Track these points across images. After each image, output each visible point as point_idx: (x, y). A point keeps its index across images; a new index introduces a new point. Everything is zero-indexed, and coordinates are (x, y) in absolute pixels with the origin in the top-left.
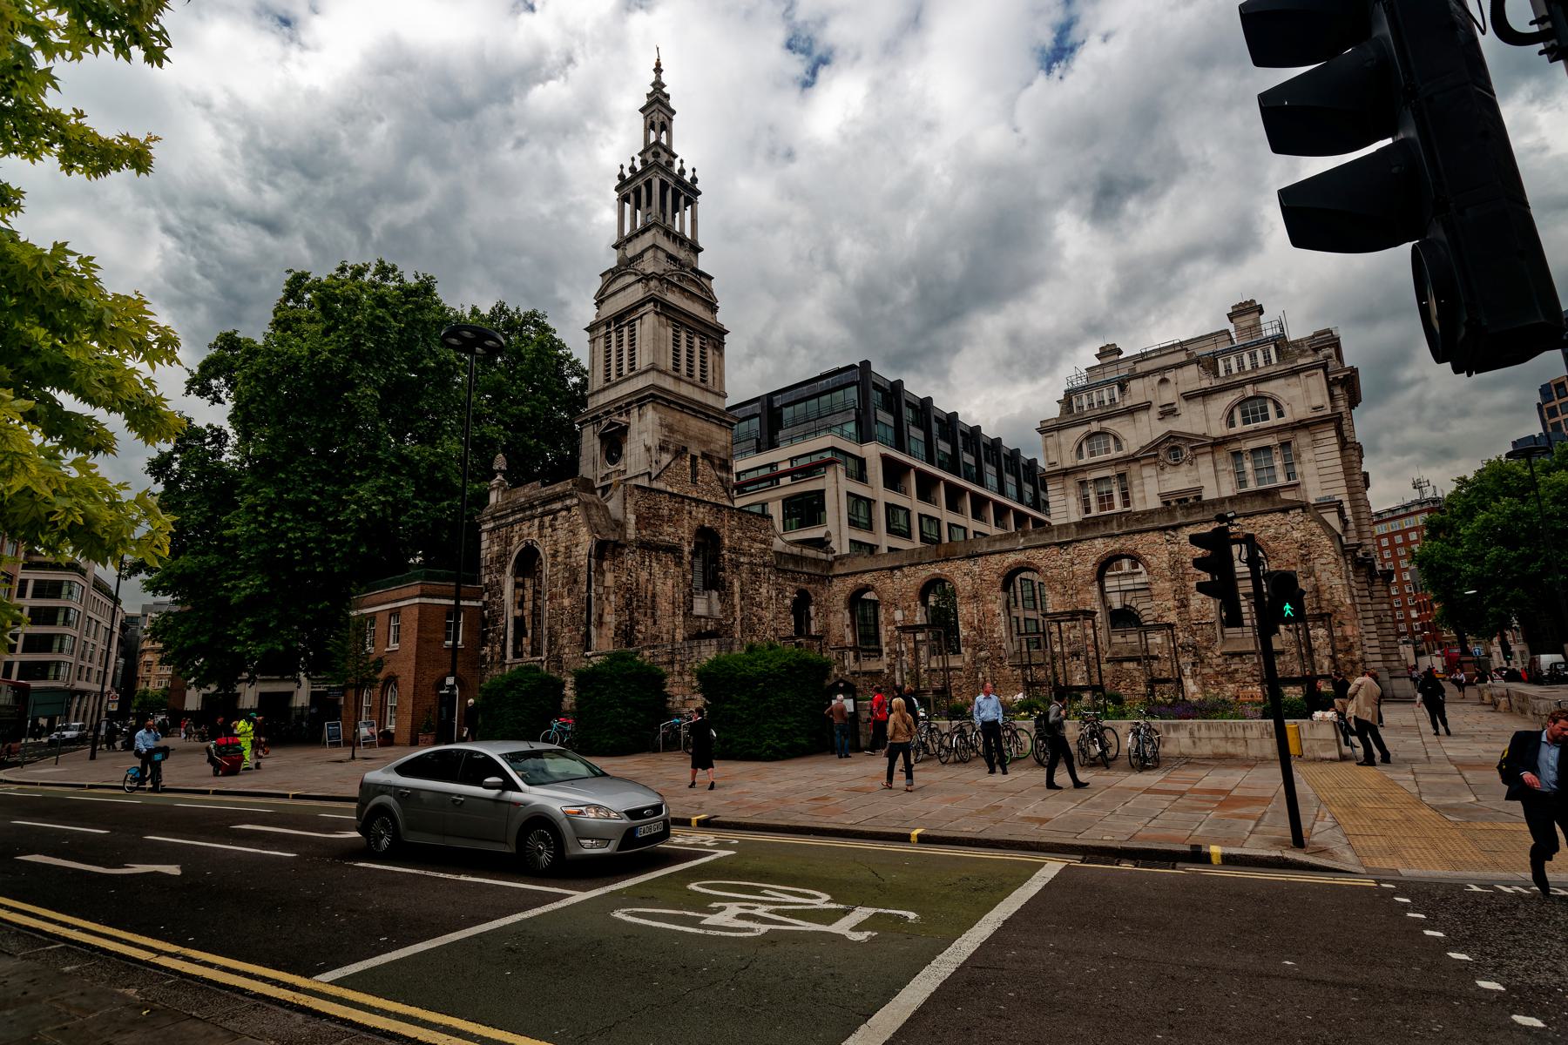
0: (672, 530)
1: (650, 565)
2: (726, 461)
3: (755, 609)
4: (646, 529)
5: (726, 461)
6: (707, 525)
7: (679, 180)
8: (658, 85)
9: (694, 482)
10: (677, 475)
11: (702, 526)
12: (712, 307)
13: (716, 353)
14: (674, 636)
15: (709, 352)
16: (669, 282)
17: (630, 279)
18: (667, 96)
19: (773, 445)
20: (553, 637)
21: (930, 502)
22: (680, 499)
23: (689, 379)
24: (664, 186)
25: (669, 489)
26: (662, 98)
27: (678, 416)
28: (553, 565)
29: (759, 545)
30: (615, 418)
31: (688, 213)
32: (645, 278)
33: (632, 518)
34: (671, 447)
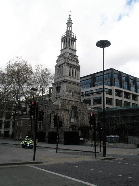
6: (74, 105)
7: (73, 38)
8: (70, 18)
9: (72, 97)
12: (78, 62)
15: (77, 71)
17: (63, 58)
18: (71, 21)
19: (94, 86)
20: (45, 126)
21: (128, 99)
23: (72, 77)
24: (69, 39)
25: (68, 99)
26: (70, 21)
28: (45, 114)
30: (59, 85)
31: (74, 43)
32: (65, 58)
33: (60, 104)
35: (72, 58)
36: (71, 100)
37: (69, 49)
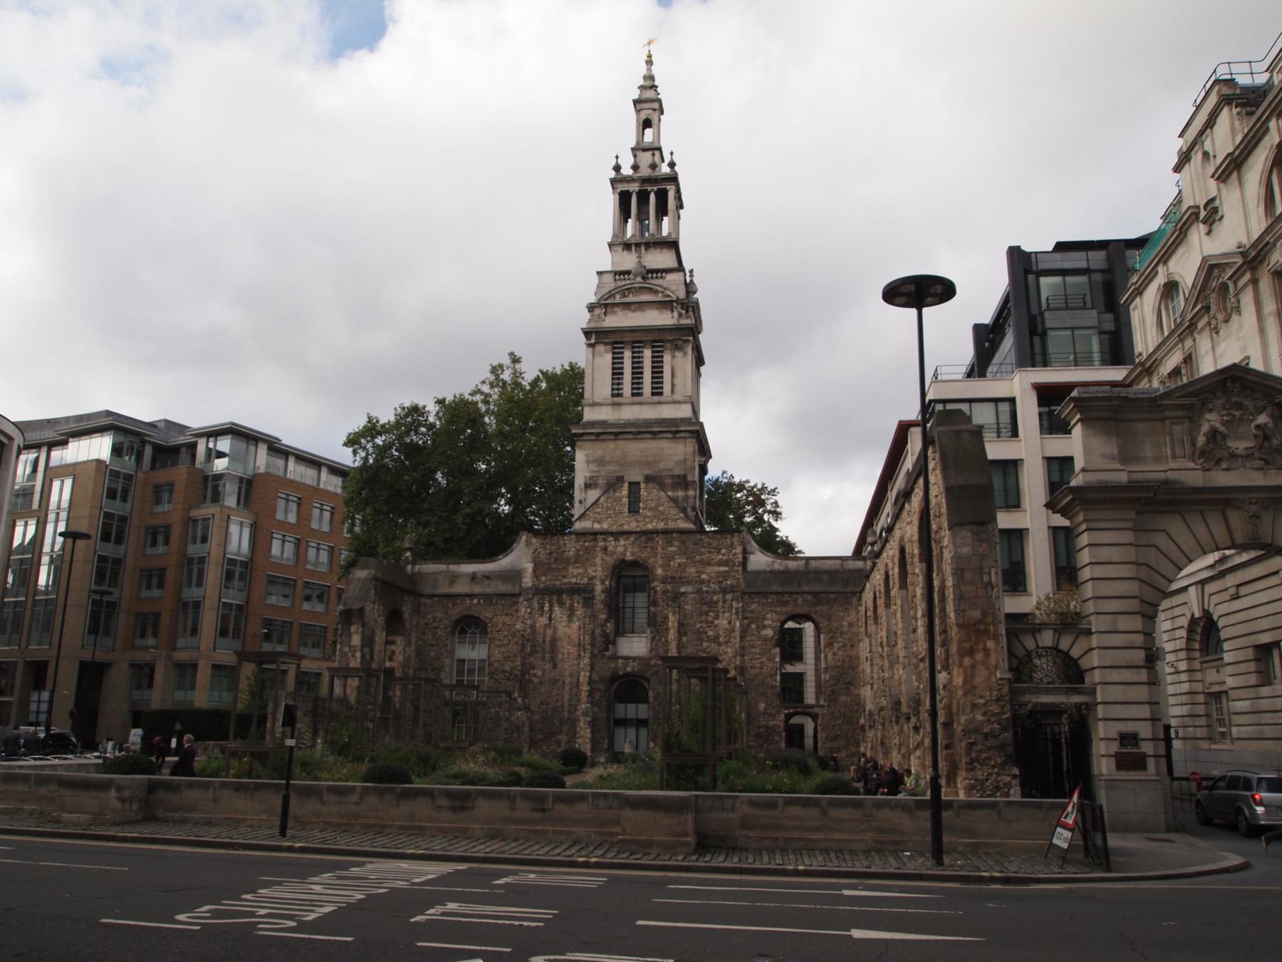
0: (581, 570)
1: (551, 610)
2: (685, 476)
3: (705, 645)
4: (545, 574)
5: (685, 476)
6: (629, 557)
8: (650, 84)
10: (608, 509)
11: (623, 561)
13: (678, 354)
14: (578, 679)
15: (667, 358)
16: (606, 305)
22: (591, 537)
25: (597, 526)
27: (611, 445)
29: (716, 569)
33: (529, 567)
34: (601, 481)
35: (626, 292)
36: (626, 528)
37: (620, 249)
